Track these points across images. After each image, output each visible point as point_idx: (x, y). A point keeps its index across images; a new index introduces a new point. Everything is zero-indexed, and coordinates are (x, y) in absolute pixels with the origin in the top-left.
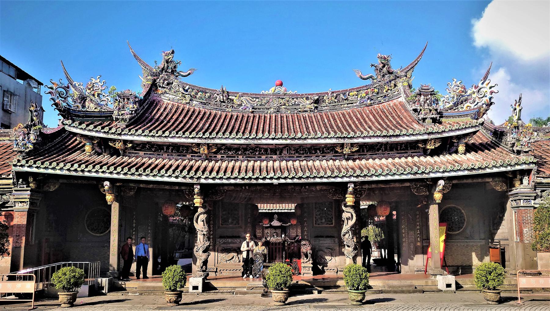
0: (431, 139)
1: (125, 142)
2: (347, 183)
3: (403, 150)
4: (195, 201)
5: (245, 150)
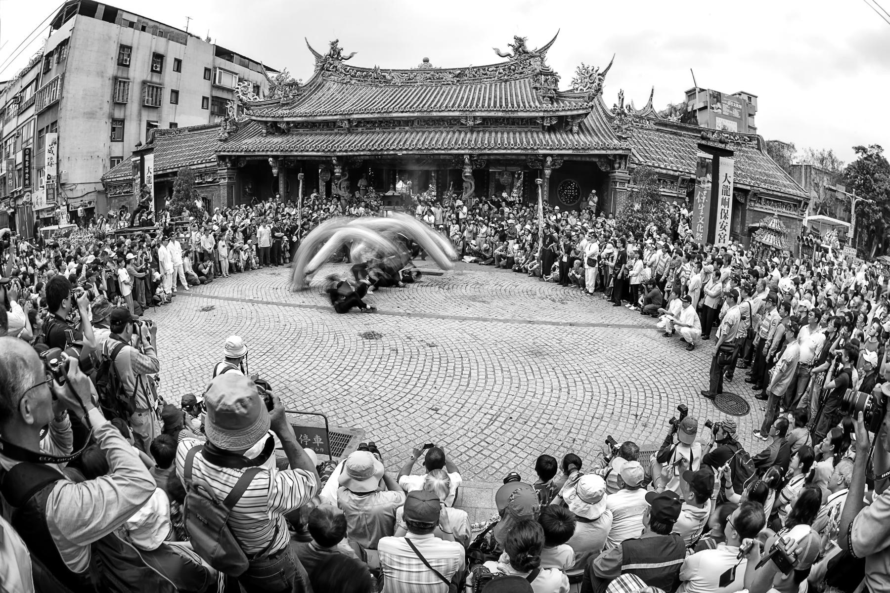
0: (547, 117)
1: (288, 123)
2: (463, 155)
3: (524, 124)
4: (335, 171)
5: (381, 122)
